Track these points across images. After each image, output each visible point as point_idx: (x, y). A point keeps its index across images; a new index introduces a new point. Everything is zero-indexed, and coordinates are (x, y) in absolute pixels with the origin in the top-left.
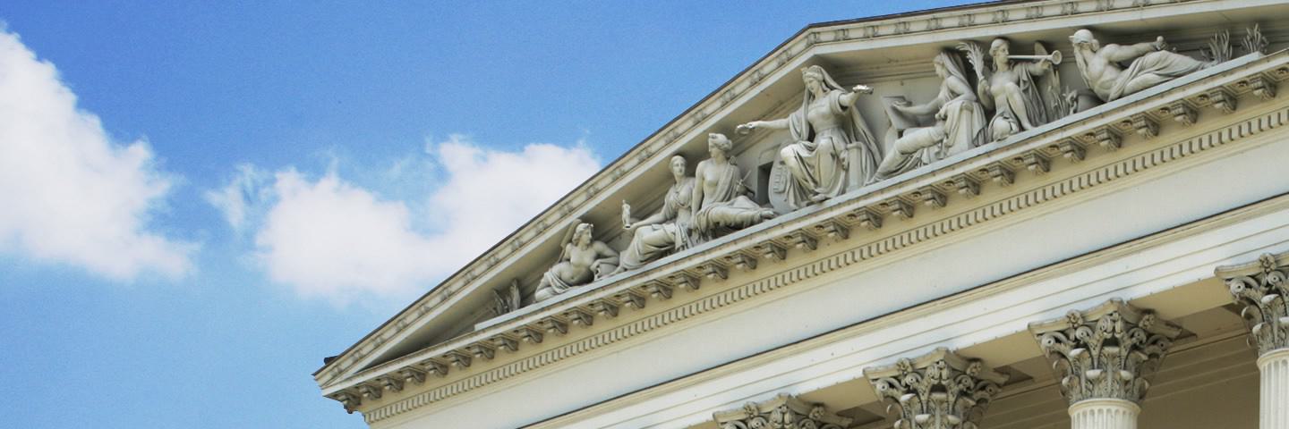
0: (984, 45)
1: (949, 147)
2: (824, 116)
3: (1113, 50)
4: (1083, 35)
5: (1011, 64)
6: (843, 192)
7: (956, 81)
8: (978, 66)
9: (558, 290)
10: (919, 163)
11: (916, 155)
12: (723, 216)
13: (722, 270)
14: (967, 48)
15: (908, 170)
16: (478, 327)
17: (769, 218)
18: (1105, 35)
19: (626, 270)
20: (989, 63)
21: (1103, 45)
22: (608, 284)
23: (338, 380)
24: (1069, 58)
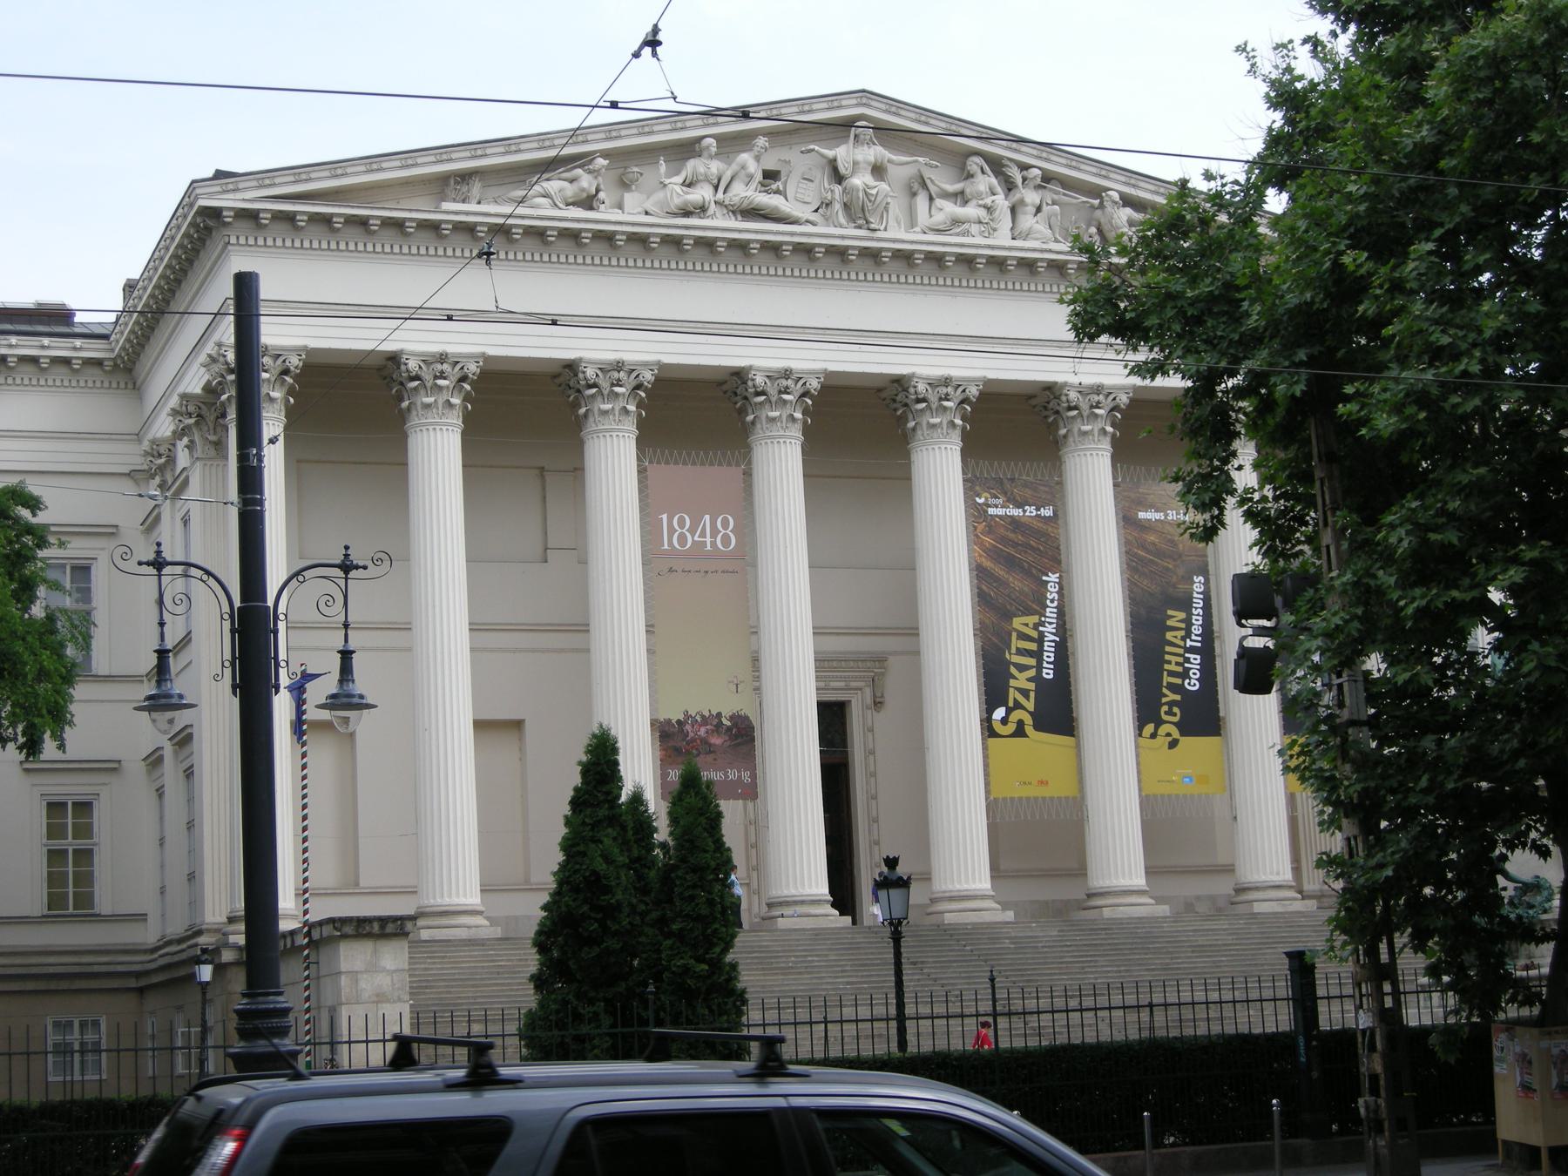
0: (1024, 167)
1: (995, 230)
2: (869, 163)
3: (1128, 211)
4: (1116, 196)
5: (1039, 187)
6: (885, 229)
7: (994, 181)
8: (1019, 181)
9: (561, 205)
10: (967, 233)
11: (966, 226)
12: (776, 209)
13: (740, 247)
14: (1008, 163)
15: (957, 234)
16: (446, 206)
17: (814, 224)
18: (1127, 201)
19: (647, 213)
20: (1024, 179)
21: (1124, 206)
22: (606, 216)
23: (231, 196)
24: (1102, 206)
